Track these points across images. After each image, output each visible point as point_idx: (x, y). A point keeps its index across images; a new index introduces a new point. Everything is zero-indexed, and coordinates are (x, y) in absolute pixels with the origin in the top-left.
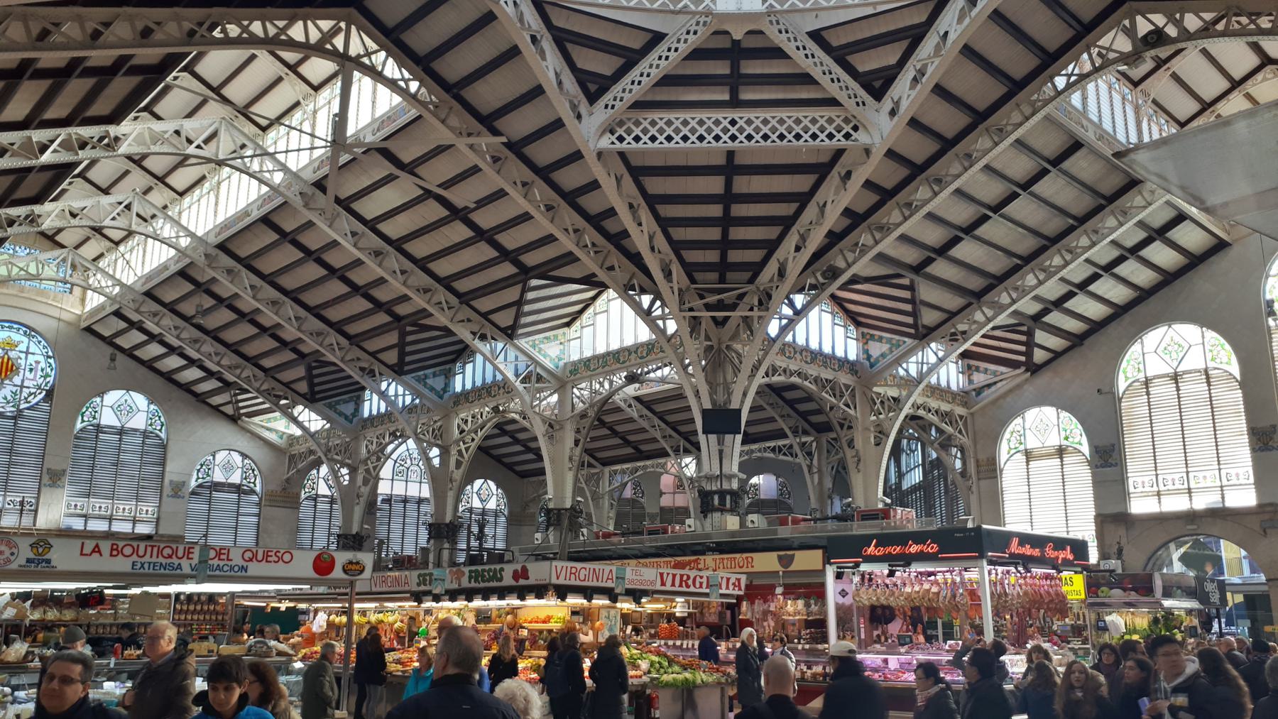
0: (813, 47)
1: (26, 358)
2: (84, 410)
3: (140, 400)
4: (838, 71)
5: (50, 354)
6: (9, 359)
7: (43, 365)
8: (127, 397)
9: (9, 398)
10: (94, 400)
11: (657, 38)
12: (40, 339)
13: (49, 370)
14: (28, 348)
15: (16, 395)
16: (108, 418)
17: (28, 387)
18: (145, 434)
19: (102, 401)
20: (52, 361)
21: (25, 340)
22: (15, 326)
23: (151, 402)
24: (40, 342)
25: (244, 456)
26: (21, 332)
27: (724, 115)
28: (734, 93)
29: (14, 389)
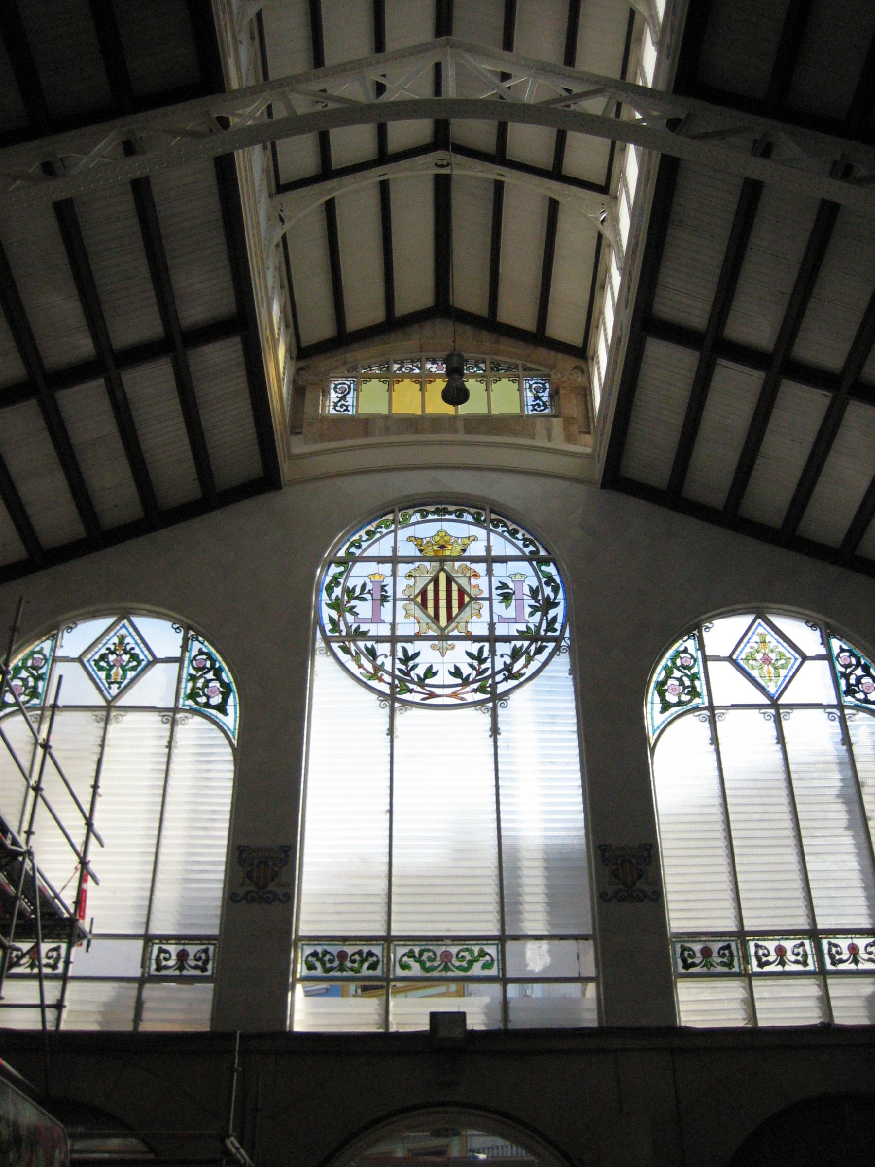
1: (490, 572)
2: (659, 675)
5: (543, 553)
6: (449, 580)
8: (762, 628)
9: (466, 671)
10: (679, 645)
12: (512, 526)
13: (548, 591)
14: (488, 548)
15: (482, 661)
17: (507, 639)
19: (701, 646)
20: (551, 569)
21: (481, 533)
22: (451, 508)
24: (514, 533)
26: (470, 519)
29: (474, 648)
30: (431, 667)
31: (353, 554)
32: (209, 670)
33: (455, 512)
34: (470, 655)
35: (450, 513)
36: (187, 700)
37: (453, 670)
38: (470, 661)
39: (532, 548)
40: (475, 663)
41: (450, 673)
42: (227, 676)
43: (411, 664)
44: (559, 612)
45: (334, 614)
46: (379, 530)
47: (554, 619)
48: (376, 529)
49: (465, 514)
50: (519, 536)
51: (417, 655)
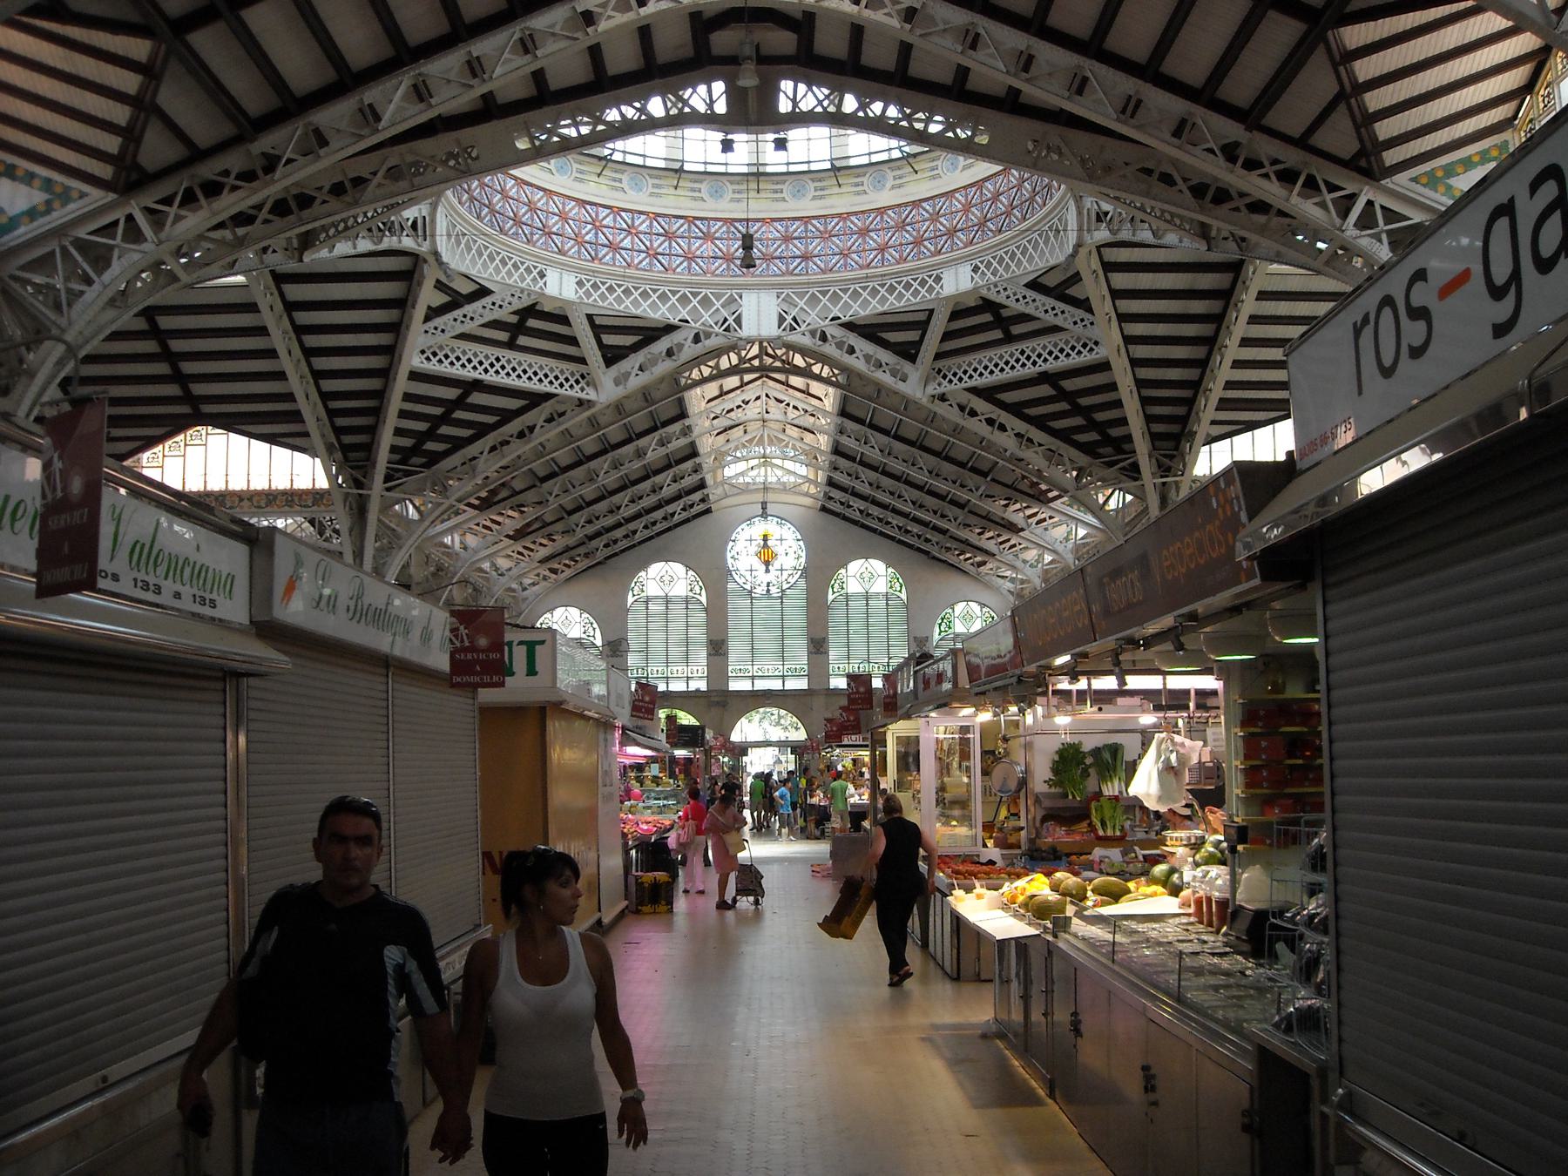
0: (1031, 294)
2: (833, 582)
3: (878, 566)
4: (1060, 306)
5: (799, 537)
7: (795, 548)
8: (867, 565)
11: (931, 311)
12: (789, 525)
16: (853, 587)
18: (887, 597)
23: (888, 565)
25: (983, 605)
26: (774, 522)
27: (1005, 351)
28: (1007, 333)
42: (701, 583)
44: (803, 560)
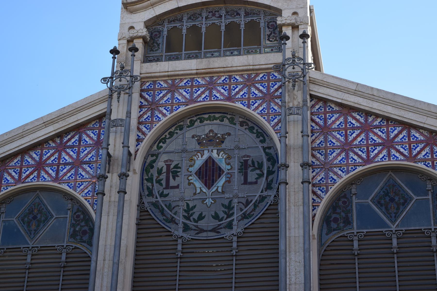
9: (221, 215)
30: (201, 214)
31: (161, 147)
32: (82, 221)
33: (218, 118)
34: (223, 205)
35: (216, 119)
36: (71, 238)
37: (214, 215)
38: (223, 209)
39: (261, 138)
40: (227, 210)
41: (213, 217)
43: (191, 212)
45: (149, 184)
46: (176, 131)
47: (272, 181)
48: (175, 131)
49: (225, 119)
50: (255, 131)
51: (194, 207)
